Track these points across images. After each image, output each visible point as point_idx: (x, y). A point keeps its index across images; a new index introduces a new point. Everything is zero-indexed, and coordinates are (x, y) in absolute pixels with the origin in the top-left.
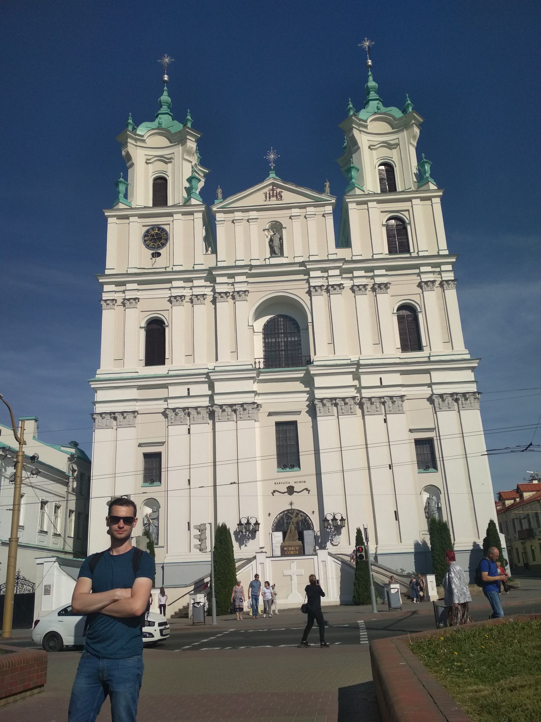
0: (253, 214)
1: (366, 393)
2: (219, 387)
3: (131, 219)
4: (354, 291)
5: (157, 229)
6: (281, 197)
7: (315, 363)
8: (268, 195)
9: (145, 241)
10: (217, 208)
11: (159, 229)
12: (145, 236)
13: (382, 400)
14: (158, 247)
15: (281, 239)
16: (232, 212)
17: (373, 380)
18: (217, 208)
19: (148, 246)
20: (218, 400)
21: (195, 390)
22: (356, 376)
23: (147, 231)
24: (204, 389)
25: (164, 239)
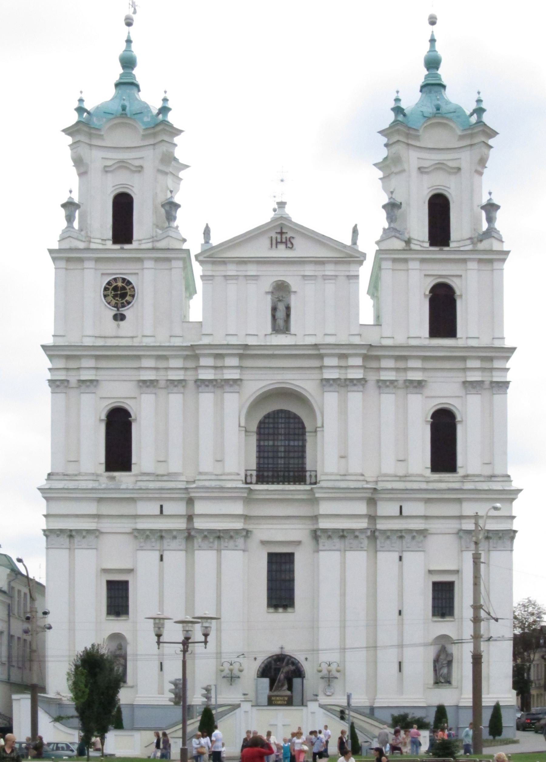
0: (252, 270)
1: (381, 525)
2: (200, 508)
3: (87, 264)
4: (379, 387)
5: (121, 280)
6: (292, 244)
7: (323, 484)
8: (274, 242)
9: (105, 296)
10: (205, 257)
11: (124, 280)
12: (106, 289)
13: (401, 535)
14: (123, 306)
15: (288, 308)
16: (224, 262)
17: (391, 509)
18: (205, 257)
19: (109, 303)
20: (199, 524)
21: (170, 508)
22: (372, 502)
23: (109, 283)
24: (180, 508)
25: (130, 295)
